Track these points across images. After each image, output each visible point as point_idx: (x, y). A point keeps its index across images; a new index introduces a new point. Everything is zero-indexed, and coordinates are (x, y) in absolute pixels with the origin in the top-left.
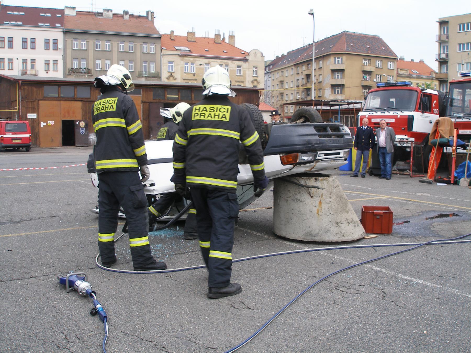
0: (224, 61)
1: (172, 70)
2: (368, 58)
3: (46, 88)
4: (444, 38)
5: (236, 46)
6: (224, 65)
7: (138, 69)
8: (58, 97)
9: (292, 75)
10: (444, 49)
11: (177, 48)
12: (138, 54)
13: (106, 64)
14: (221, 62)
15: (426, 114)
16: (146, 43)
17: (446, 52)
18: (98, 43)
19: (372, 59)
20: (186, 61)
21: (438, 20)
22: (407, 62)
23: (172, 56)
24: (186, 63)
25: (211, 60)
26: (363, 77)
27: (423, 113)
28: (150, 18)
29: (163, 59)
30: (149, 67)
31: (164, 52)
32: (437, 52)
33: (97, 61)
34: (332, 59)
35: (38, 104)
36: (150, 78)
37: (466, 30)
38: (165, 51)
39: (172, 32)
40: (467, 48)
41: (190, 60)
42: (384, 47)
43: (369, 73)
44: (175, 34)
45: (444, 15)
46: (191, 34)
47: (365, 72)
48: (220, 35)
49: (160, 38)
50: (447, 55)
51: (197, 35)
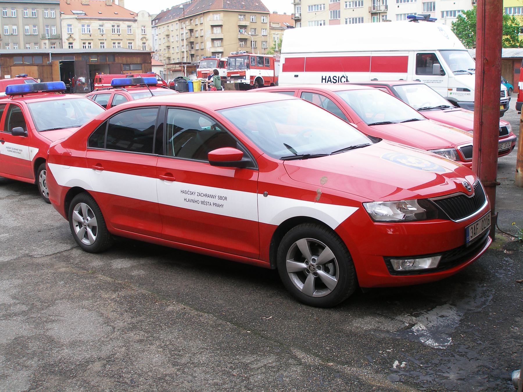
2: (243, 14)
3: (15, 58)
5: (126, 6)
7: (42, 32)
8: (23, 64)
9: (177, 30)
10: (298, 10)
11: (74, 12)
12: (41, 19)
13: (13, 29)
16: (46, 9)
18: (5, 11)
19: (247, 15)
22: (280, 15)
23: (70, 20)
24: (83, 26)
25: (105, 22)
26: (240, 31)
29: (62, 23)
30: (51, 30)
33: (5, 26)
34: (210, 16)
35: (11, 69)
42: (257, 3)
43: (245, 27)
47: (241, 27)
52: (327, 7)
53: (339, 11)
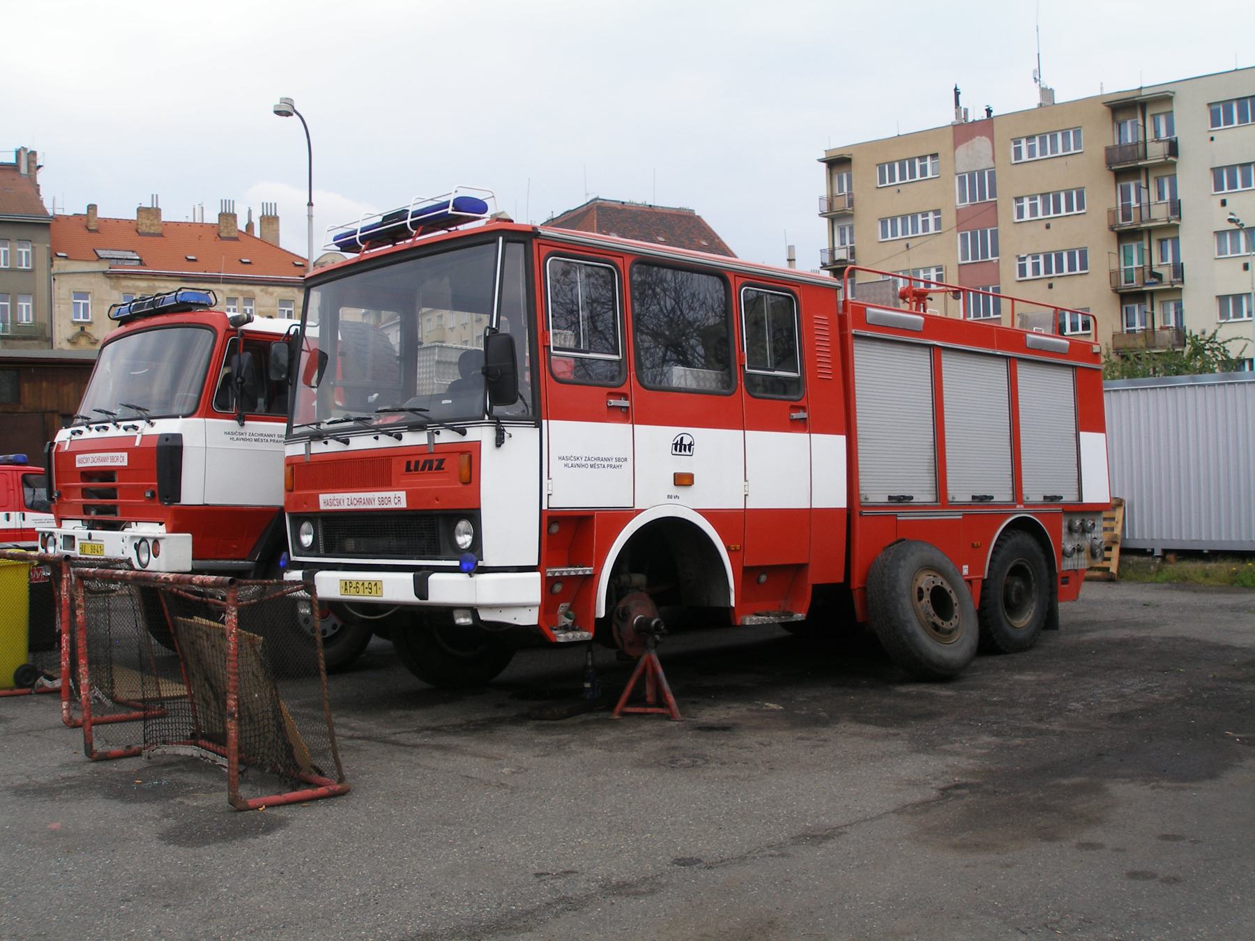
0: (240, 287)
1: (86, 316)
4: (840, 204)
5: (282, 246)
6: (241, 299)
9: (464, 326)
10: (842, 236)
11: (101, 253)
14: (231, 291)
15: (253, 426)
17: (848, 244)
20: (127, 290)
21: (823, 156)
23: (85, 278)
27: (241, 419)
28: (24, 169)
29: (56, 285)
31: (59, 265)
32: (826, 245)
36: (16, 343)
37: (897, 181)
38: (63, 262)
39: (92, 208)
40: (905, 231)
41: (137, 288)
42: (705, 239)
44: (101, 214)
45: (839, 142)
46: (149, 213)
48: (234, 216)
49: (46, 226)
50: (853, 254)
51: (165, 217)
52: (949, 219)
53: (995, 234)
